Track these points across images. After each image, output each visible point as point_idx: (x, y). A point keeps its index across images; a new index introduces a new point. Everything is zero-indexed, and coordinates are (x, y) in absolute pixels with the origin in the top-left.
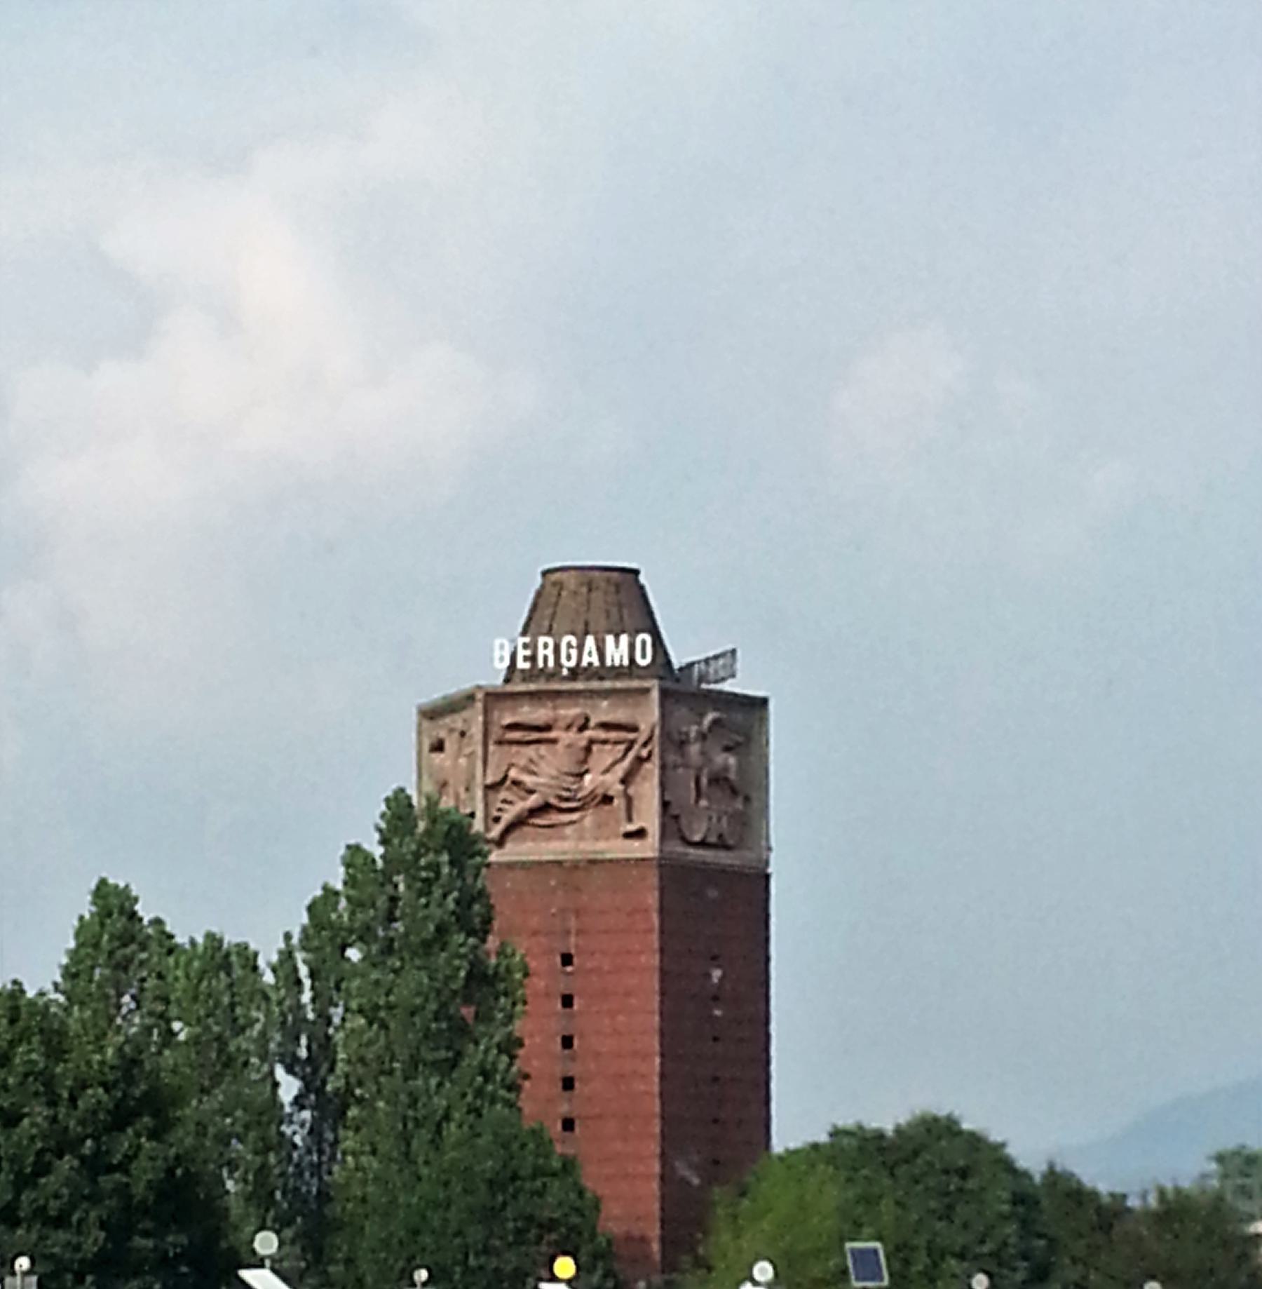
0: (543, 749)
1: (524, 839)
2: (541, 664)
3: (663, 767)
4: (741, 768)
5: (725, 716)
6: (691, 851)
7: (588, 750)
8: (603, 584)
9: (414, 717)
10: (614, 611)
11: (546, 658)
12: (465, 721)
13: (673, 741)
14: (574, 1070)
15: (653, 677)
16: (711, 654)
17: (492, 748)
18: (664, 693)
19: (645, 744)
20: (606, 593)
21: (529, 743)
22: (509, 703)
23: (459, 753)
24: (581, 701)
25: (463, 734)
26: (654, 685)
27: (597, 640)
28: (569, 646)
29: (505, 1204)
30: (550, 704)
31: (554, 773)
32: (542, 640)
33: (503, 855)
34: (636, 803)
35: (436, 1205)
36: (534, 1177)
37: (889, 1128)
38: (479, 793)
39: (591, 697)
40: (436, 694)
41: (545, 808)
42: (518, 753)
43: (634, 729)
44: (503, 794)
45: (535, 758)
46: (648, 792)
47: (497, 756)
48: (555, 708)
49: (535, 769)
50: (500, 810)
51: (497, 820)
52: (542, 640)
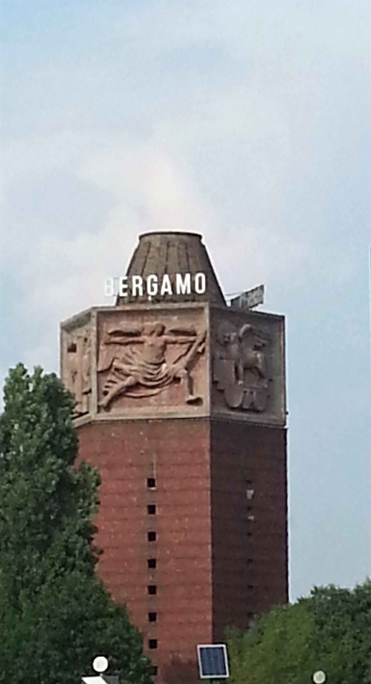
0: (135, 348)
1: (122, 405)
2: (134, 294)
3: (213, 359)
4: (265, 360)
5: (254, 327)
6: (232, 413)
7: (164, 348)
8: (177, 244)
9: (59, 330)
10: (184, 260)
11: (137, 290)
12: (87, 331)
13: (220, 343)
14: (157, 554)
15: (205, 301)
16: (249, 289)
17: (102, 348)
18: (211, 309)
19: (200, 344)
20: (179, 248)
21: (127, 344)
22: (113, 318)
23: (84, 353)
24: (161, 317)
25: (86, 340)
26: (206, 305)
27: (170, 279)
28: (152, 281)
29: (75, 636)
30: (140, 318)
31: (142, 363)
32: (134, 278)
33: (108, 416)
34: (195, 381)
35: (27, 637)
36: (96, 617)
37: (352, 588)
38: (94, 376)
39: (166, 314)
40: (68, 316)
41: (137, 385)
42: (119, 350)
43: (195, 334)
44: (110, 377)
45: (130, 354)
46: (203, 375)
47: (105, 354)
48: (143, 321)
49: (131, 361)
50: (107, 387)
51: (106, 393)
52: (134, 278)
